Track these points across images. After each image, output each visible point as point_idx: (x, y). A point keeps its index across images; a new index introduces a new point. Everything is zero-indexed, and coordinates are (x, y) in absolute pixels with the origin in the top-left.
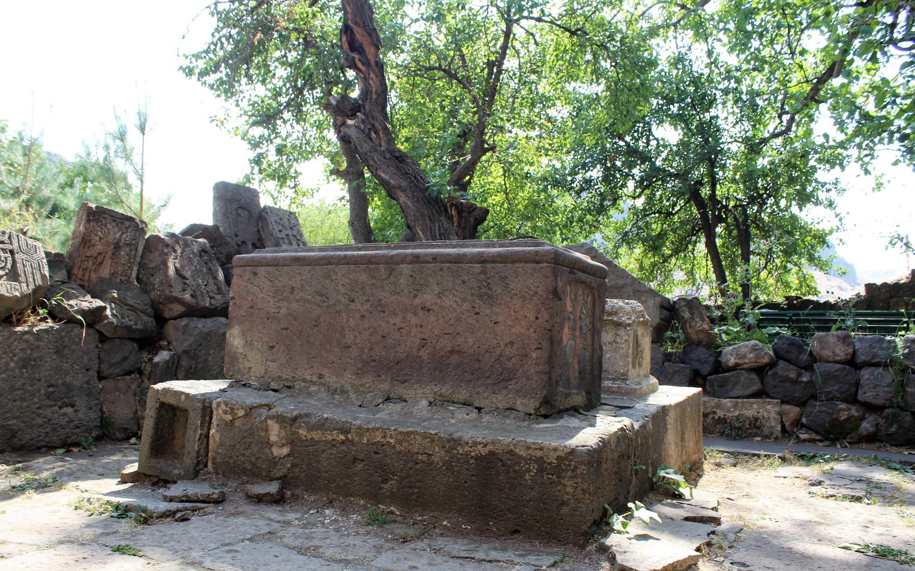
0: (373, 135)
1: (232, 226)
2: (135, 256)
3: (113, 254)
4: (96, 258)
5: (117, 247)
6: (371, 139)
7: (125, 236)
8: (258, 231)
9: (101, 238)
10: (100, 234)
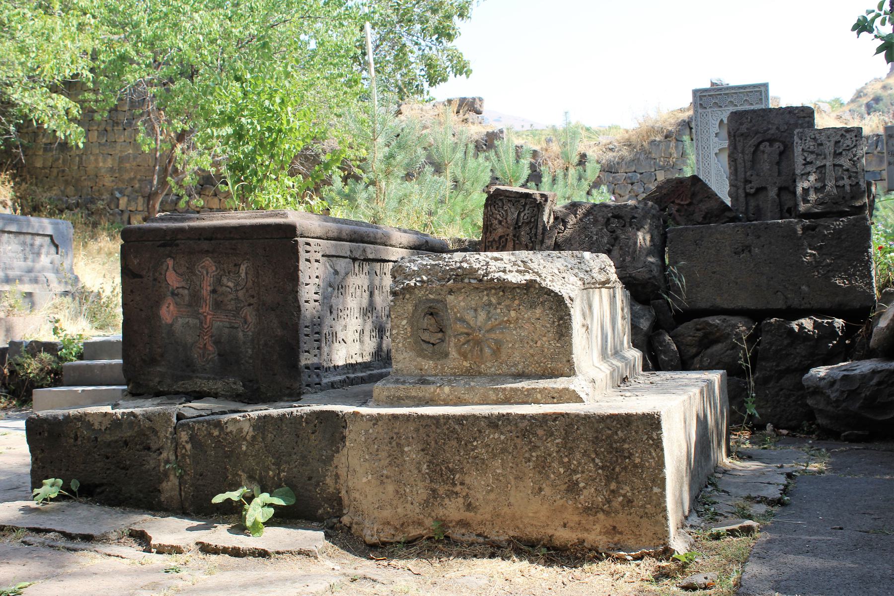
2: (536, 235)
3: (514, 236)
5: (517, 227)
7: (522, 215)
9: (500, 222)
10: (498, 216)
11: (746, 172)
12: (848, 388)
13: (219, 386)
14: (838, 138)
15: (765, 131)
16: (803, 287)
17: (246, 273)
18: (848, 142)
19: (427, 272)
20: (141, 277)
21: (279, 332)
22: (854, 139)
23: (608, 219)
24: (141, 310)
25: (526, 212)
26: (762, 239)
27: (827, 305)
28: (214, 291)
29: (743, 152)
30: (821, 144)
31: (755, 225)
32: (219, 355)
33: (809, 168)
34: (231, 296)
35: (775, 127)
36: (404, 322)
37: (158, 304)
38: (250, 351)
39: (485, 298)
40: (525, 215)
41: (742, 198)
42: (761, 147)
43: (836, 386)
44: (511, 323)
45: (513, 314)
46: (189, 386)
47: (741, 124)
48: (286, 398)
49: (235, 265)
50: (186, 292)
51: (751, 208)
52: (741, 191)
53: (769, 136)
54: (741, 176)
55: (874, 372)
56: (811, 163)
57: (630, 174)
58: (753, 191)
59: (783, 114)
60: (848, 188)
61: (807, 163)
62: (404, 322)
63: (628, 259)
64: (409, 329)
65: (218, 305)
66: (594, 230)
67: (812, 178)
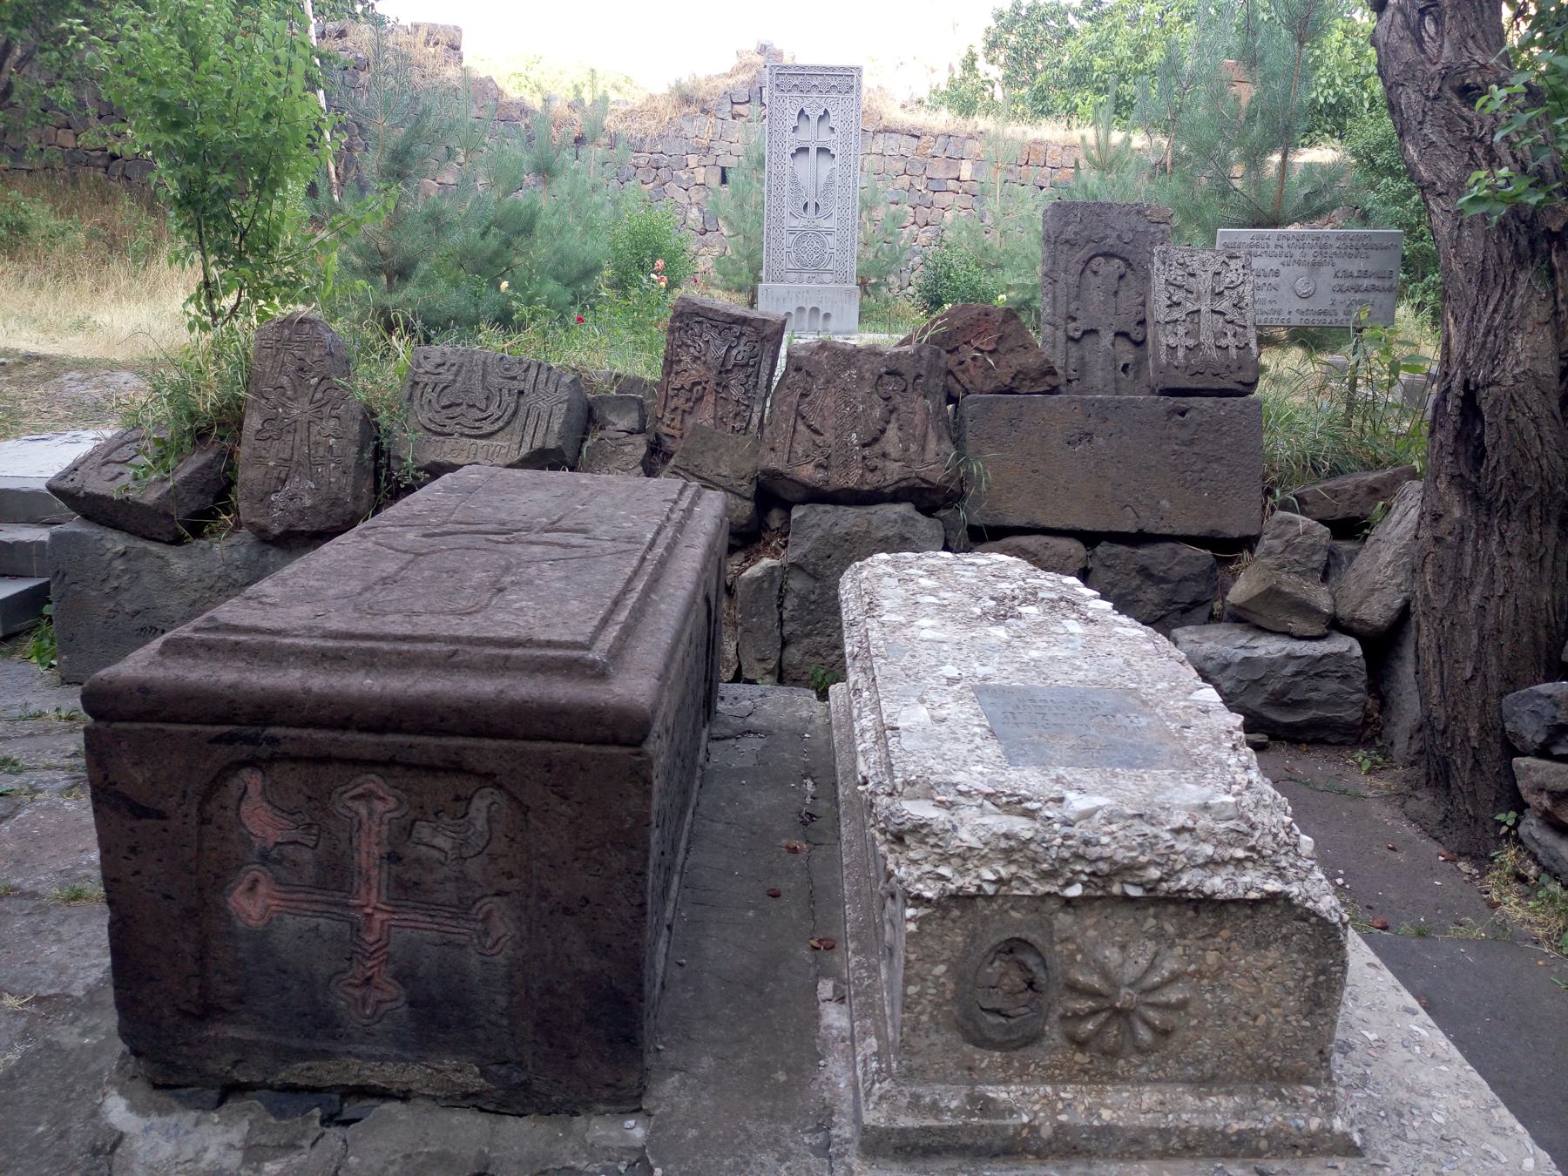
0: (1430, 28)
1: (1062, 300)
3: (718, 384)
4: (691, 390)
5: (724, 371)
6: (1420, 41)
7: (734, 352)
8: (1143, 304)
11: (1068, 304)
12: (1249, 676)
13: (413, 1075)
14: (1217, 267)
15: (1102, 239)
16: (1164, 502)
17: (489, 820)
18: (1232, 276)
19: (1008, 855)
20: (161, 815)
21: (588, 963)
22: (1241, 271)
23: (880, 377)
24: (167, 897)
25: (741, 348)
26: (1110, 423)
27: (1194, 532)
28: (393, 858)
29: (1065, 271)
30: (1193, 275)
31: (1100, 401)
32: (411, 1004)
33: (1177, 314)
34: (442, 872)
35: (1115, 235)
36: (940, 969)
37: (221, 880)
38: (502, 1001)
39: (1151, 922)
40: (741, 351)
41: (1060, 347)
42: (1094, 264)
43: (1229, 672)
44: (1202, 977)
45: (1211, 957)
46: (327, 1073)
47: (1067, 224)
48: (602, 1108)
49: (457, 798)
50: (307, 855)
51: (1072, 360)
52: (1060, 333)
53: (1106, 249)
54: (1062, 310)
55: (1290, 657)
56: (1179, 304)
57: (656, 156)
58: (1078, 334)
59: (1128, 214)
60: (1233, 352)
61: (1175, 304)
62: (940, 969)
63: (913, 447)
64: (951, 986)
65: (406, 890)
66: (860, 394)
67: (1181, 330)
